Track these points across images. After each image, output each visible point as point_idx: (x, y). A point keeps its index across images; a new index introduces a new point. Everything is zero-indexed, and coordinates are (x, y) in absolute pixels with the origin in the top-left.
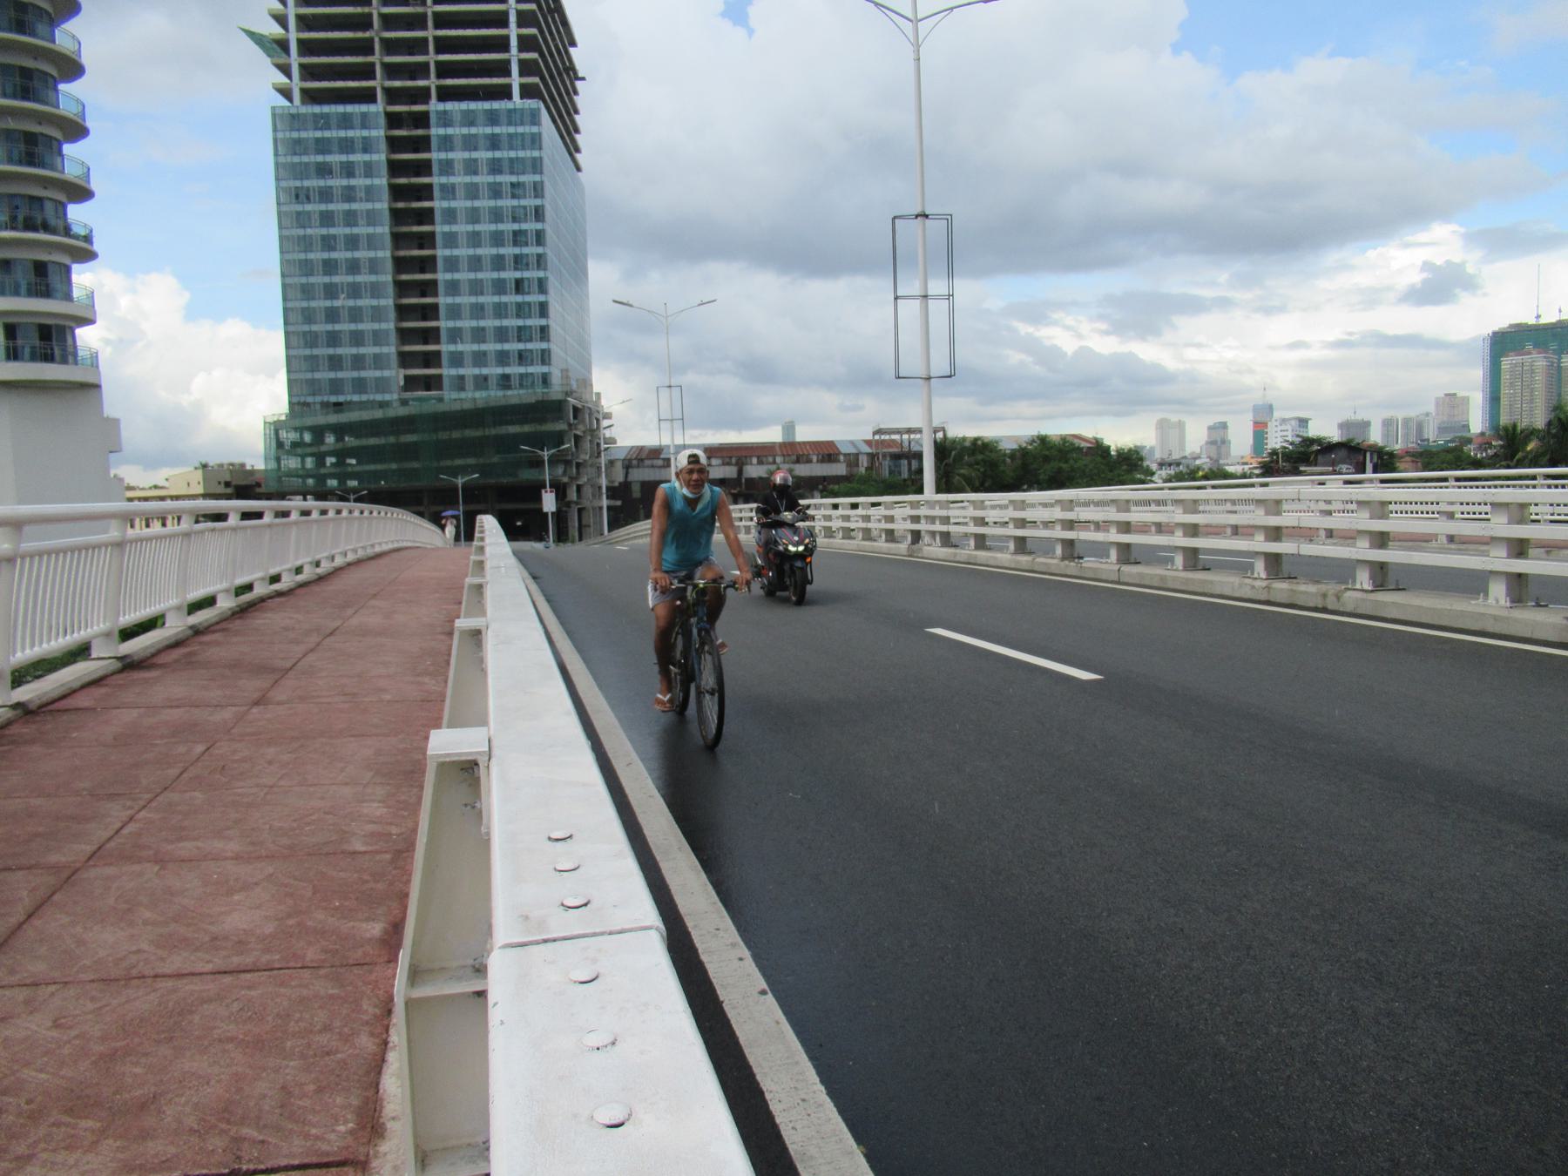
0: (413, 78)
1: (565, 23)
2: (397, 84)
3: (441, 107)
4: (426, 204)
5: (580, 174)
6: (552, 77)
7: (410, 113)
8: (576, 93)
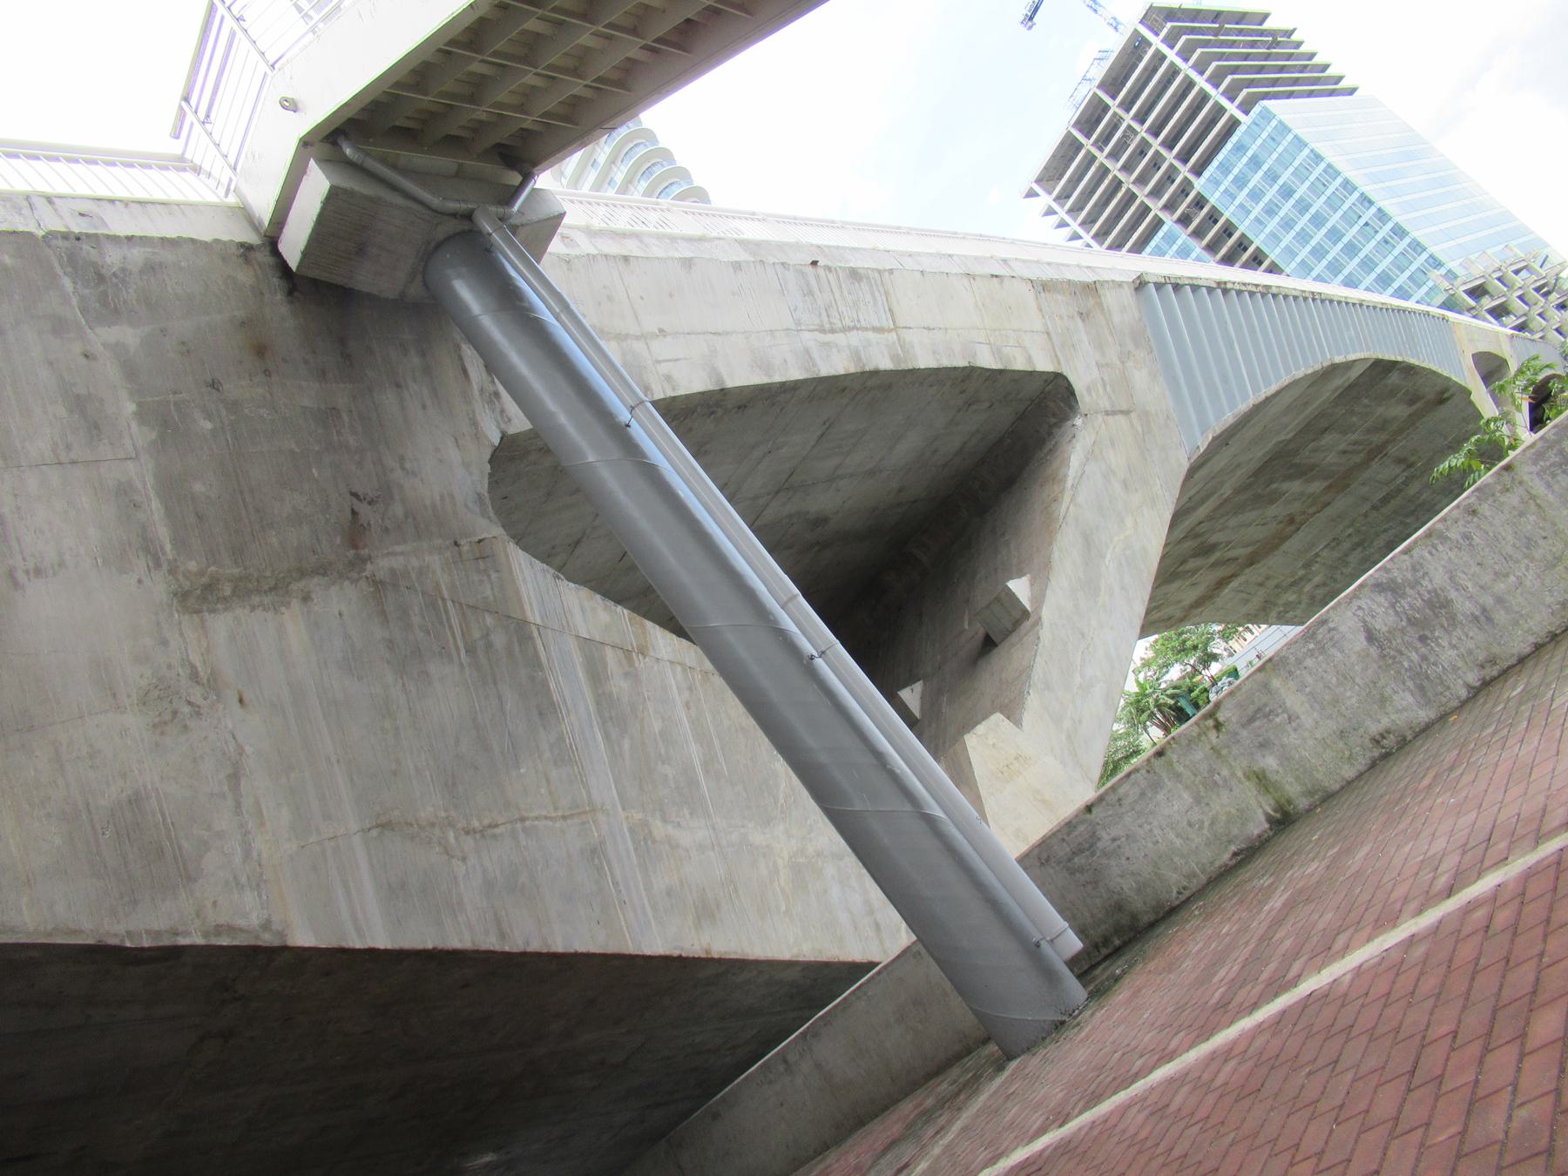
0: (1173, 181)
1: (1241, 17)
2: (1166, 197)
3: (1202, 180)
4: (1251, 250)
5: (1356, 93)
6: (1260, 70)
7: (1188, 207)
8: (1299, 44)
